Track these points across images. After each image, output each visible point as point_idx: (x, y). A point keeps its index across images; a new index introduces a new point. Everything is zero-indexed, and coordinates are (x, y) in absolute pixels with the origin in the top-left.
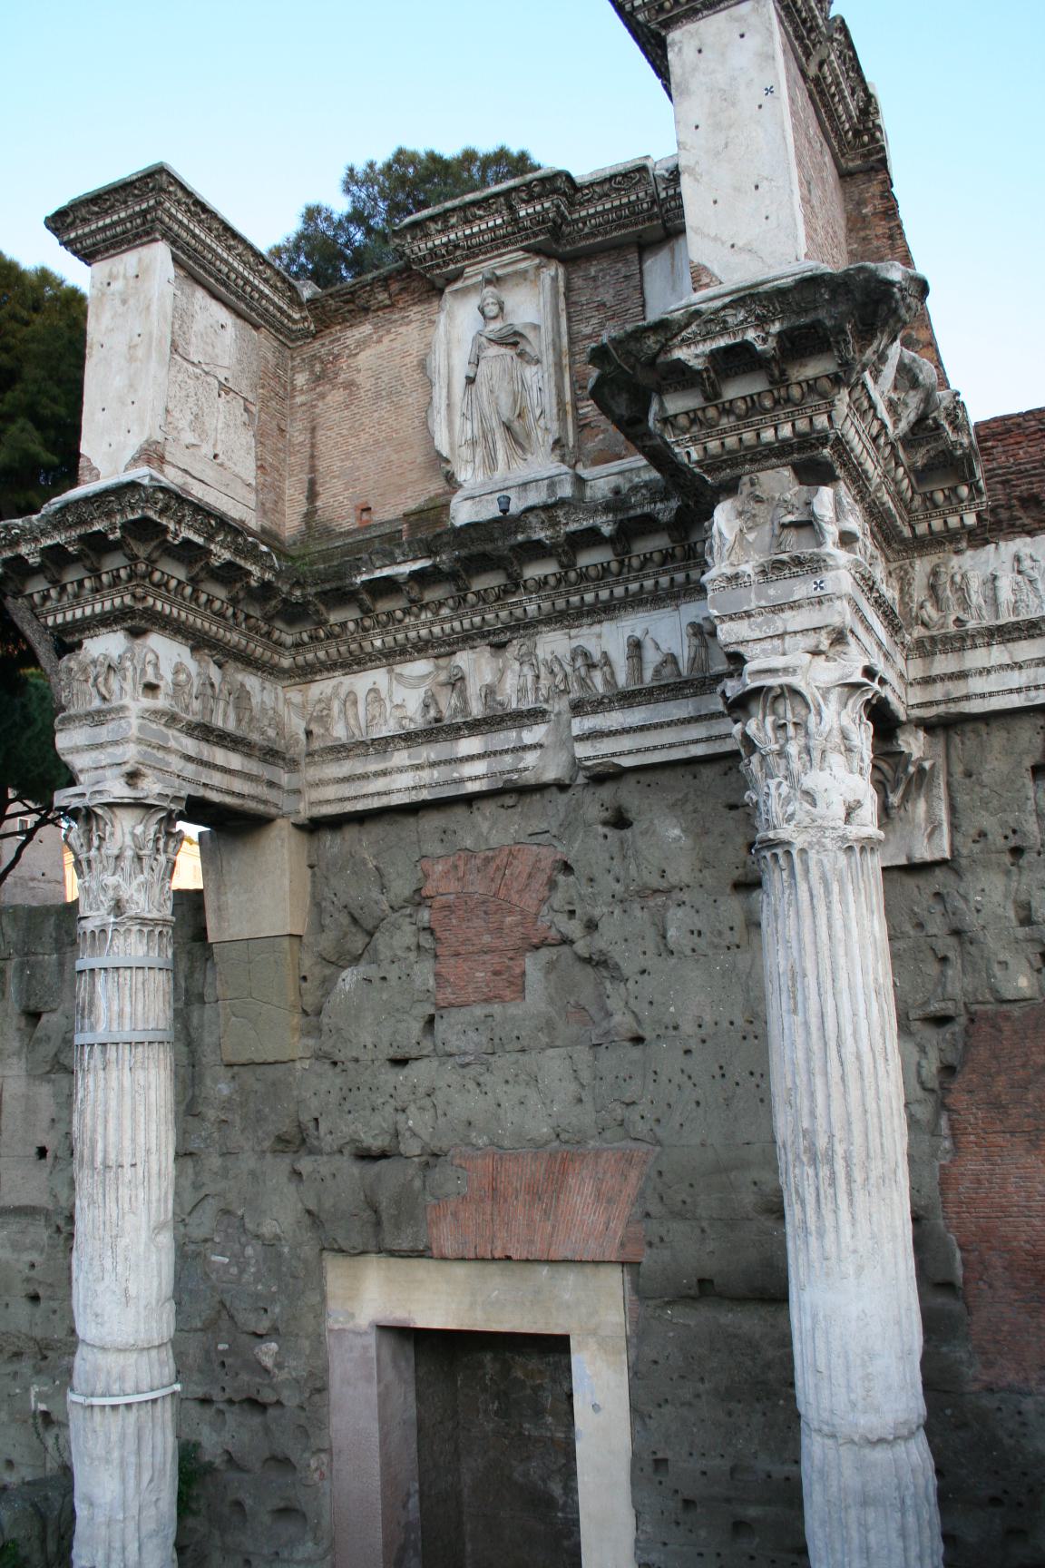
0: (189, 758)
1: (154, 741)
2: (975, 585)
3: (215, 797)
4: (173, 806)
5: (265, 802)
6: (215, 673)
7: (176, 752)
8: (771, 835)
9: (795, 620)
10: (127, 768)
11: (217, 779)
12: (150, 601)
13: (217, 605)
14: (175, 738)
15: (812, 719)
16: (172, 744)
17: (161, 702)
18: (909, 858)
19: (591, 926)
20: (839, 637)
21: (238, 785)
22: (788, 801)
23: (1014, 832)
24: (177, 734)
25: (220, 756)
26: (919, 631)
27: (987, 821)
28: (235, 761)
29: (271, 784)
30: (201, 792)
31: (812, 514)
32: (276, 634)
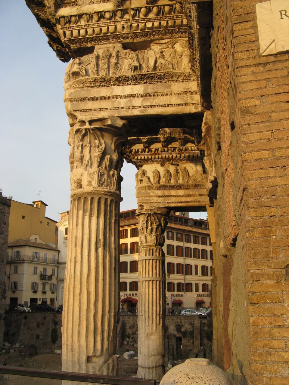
0: (160, 197)
1: (144, 195)
3: (173, 205)
4: (150, 212)
5: (199, 202)
6: (172, 169)
7: (154, 196)
11: (173, 199)
12: (136, 158)
13: (160, 149)
14: (152, 192)
16: (152, 194)
17: (144, 184)
21: (183, 199)
24: (153, 191)
25: (173, 192)
28: (181, 192)
29: (201, 195)
30: (167, 205)
32: (190, 148)
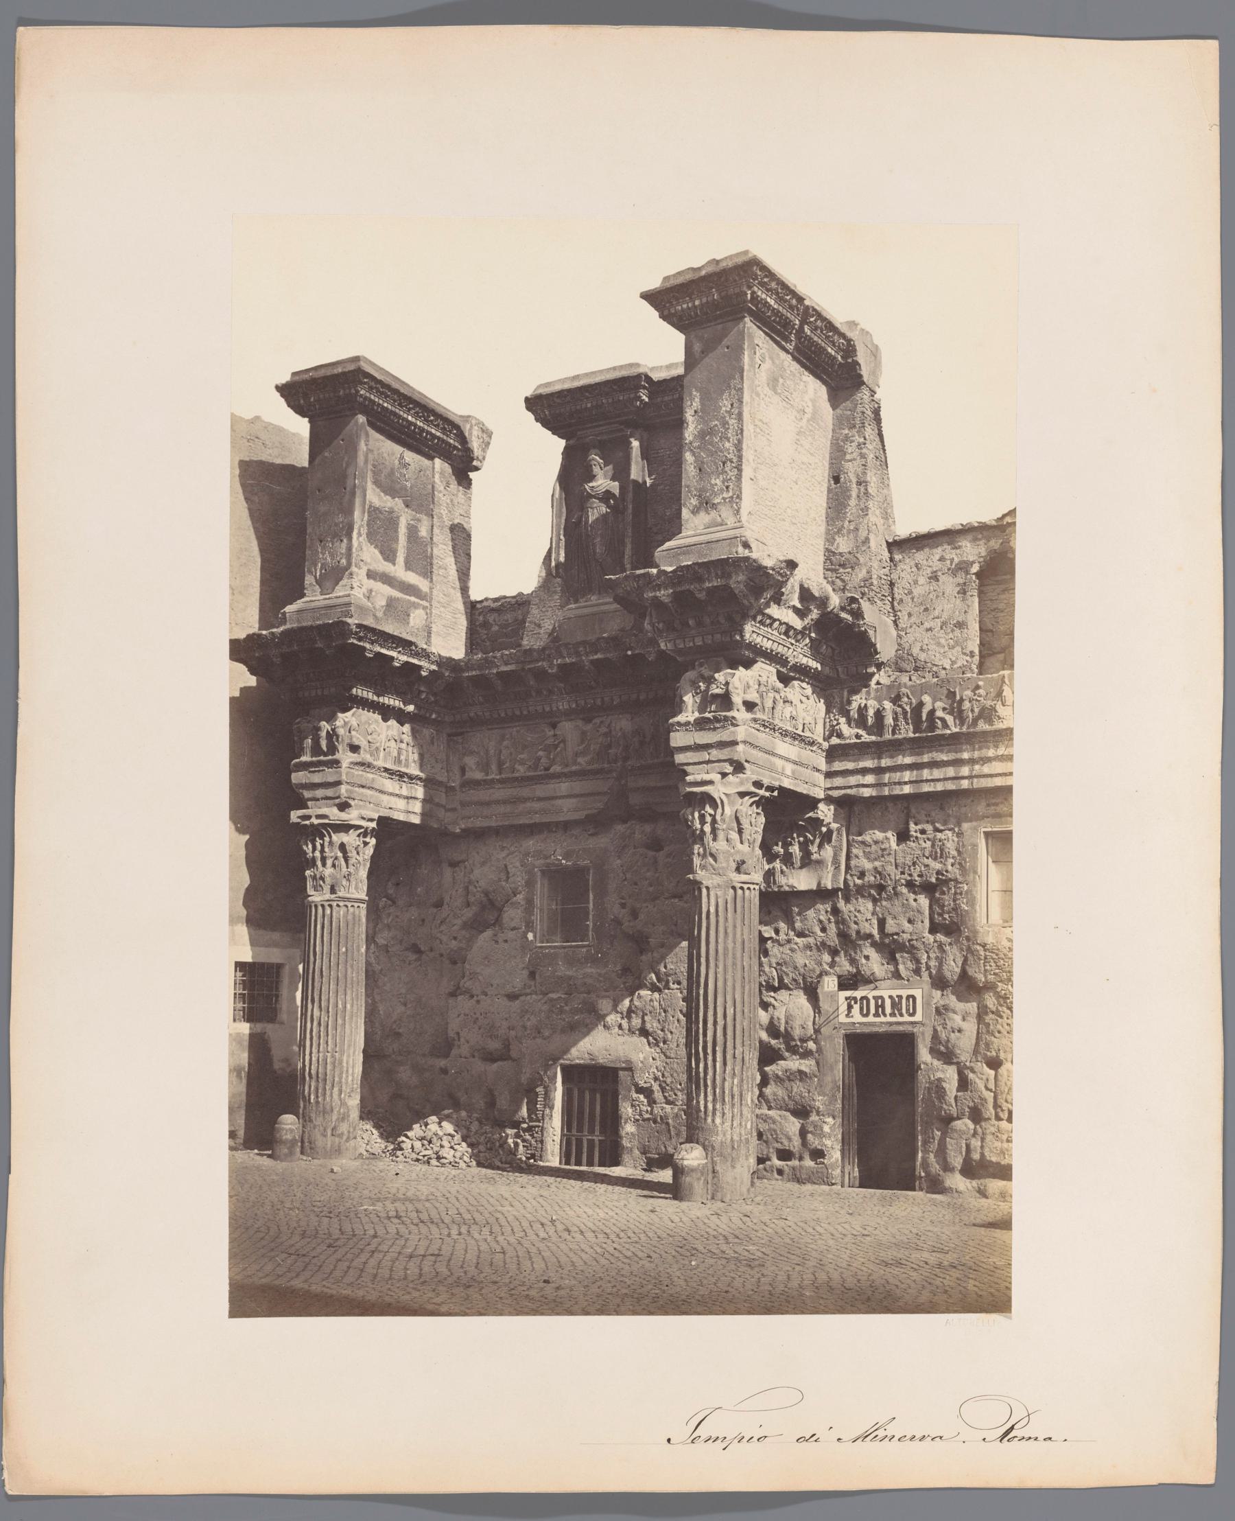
2: (871, 712)
8: (691, 876)
9: (715, 754)
10: (337, 801)
15: (719, 810)
18: (819, 884)
19: (634, 914)
20: (739, 767)
22: (704, 856)
23: (880, 874)
26: (835, 741)
27: (868, 865)
31: (727, 690)
